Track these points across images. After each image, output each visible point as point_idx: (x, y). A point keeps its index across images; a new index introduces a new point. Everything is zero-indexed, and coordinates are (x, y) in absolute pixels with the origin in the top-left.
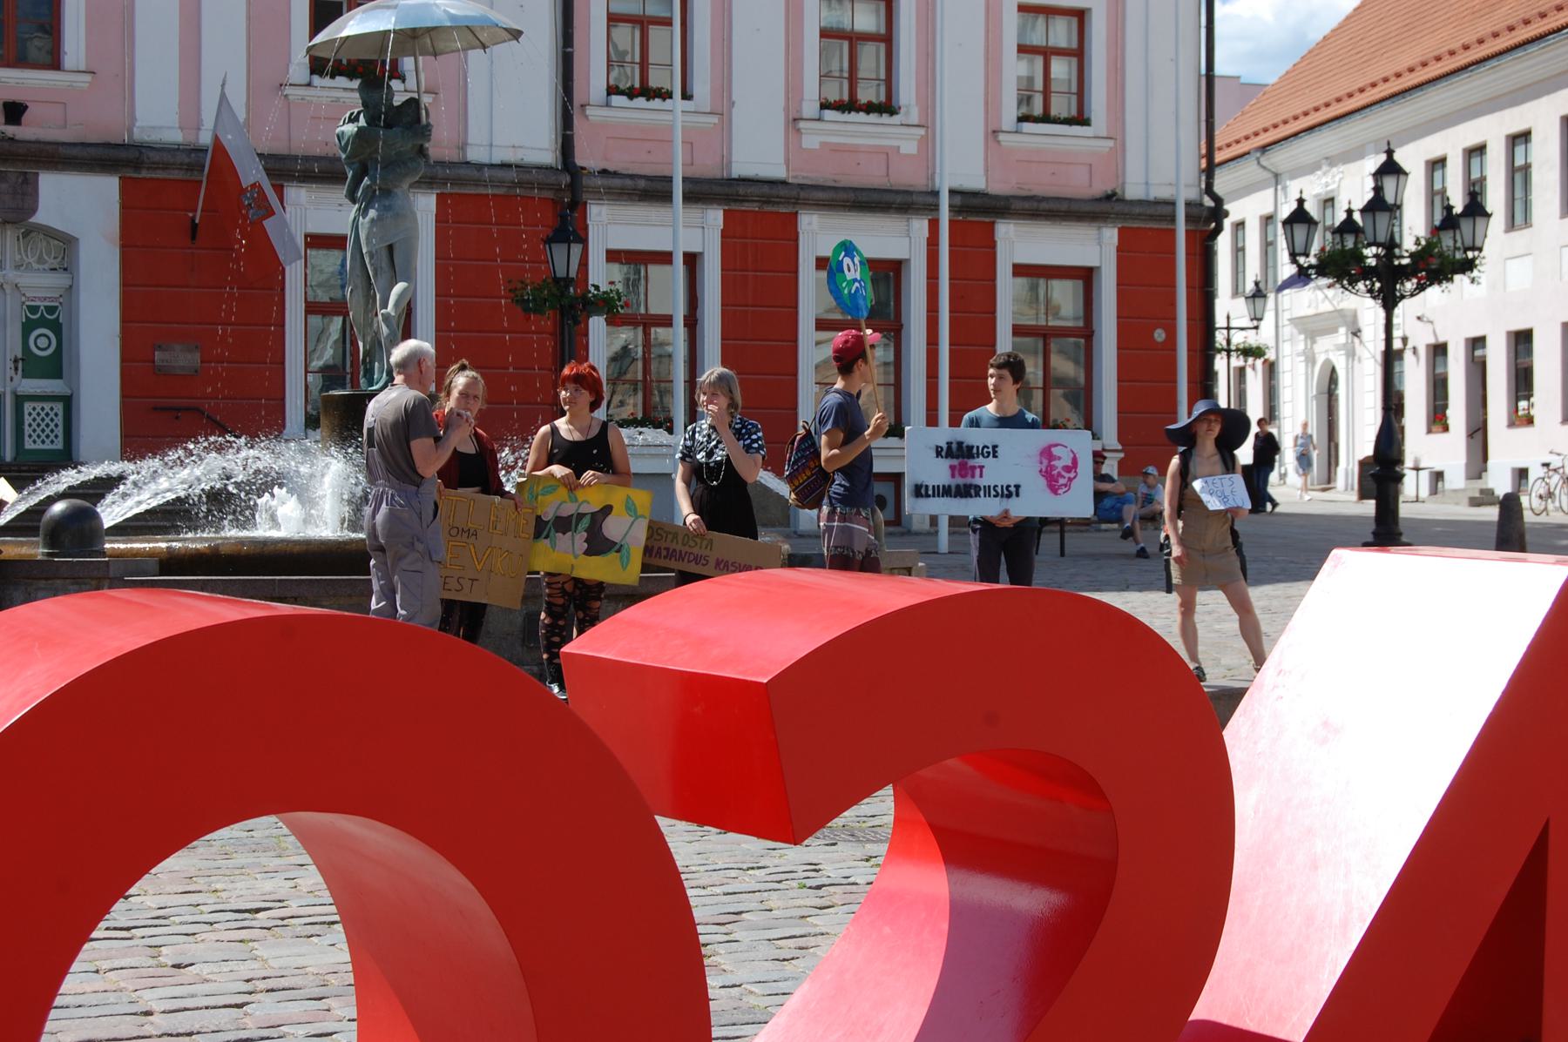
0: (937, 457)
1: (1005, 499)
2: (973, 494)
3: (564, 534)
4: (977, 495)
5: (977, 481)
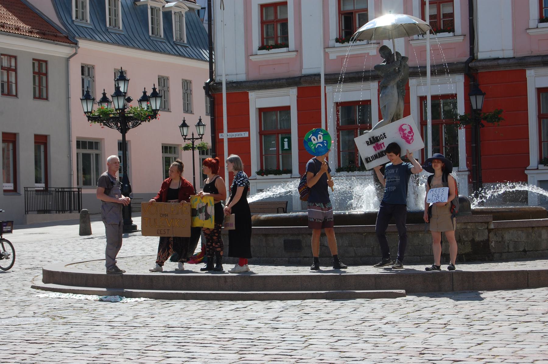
2: (384, 154)
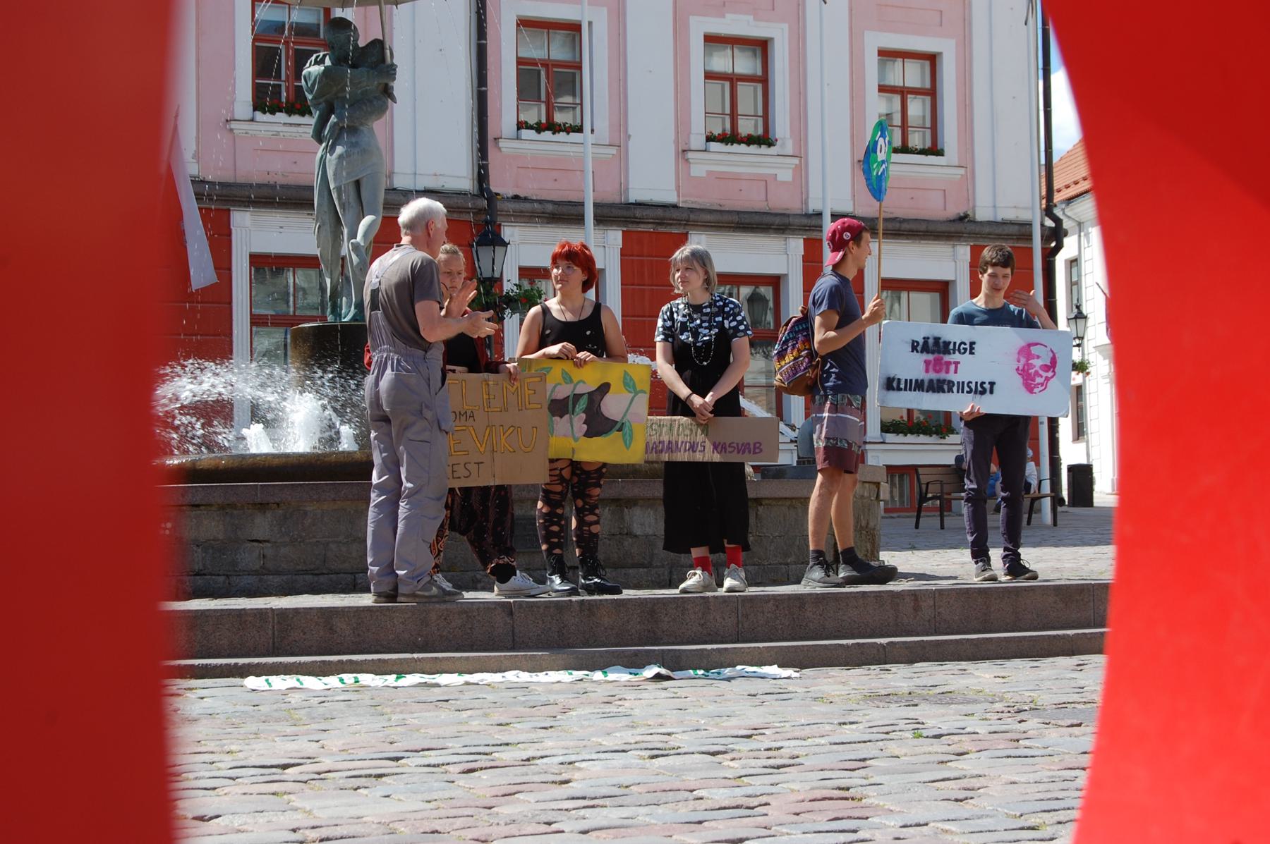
0: (912, 351)
1: (978, 396)
2: (946, 390)
3: (561, 417)
4: (950, 390)
5: (951, 376)
